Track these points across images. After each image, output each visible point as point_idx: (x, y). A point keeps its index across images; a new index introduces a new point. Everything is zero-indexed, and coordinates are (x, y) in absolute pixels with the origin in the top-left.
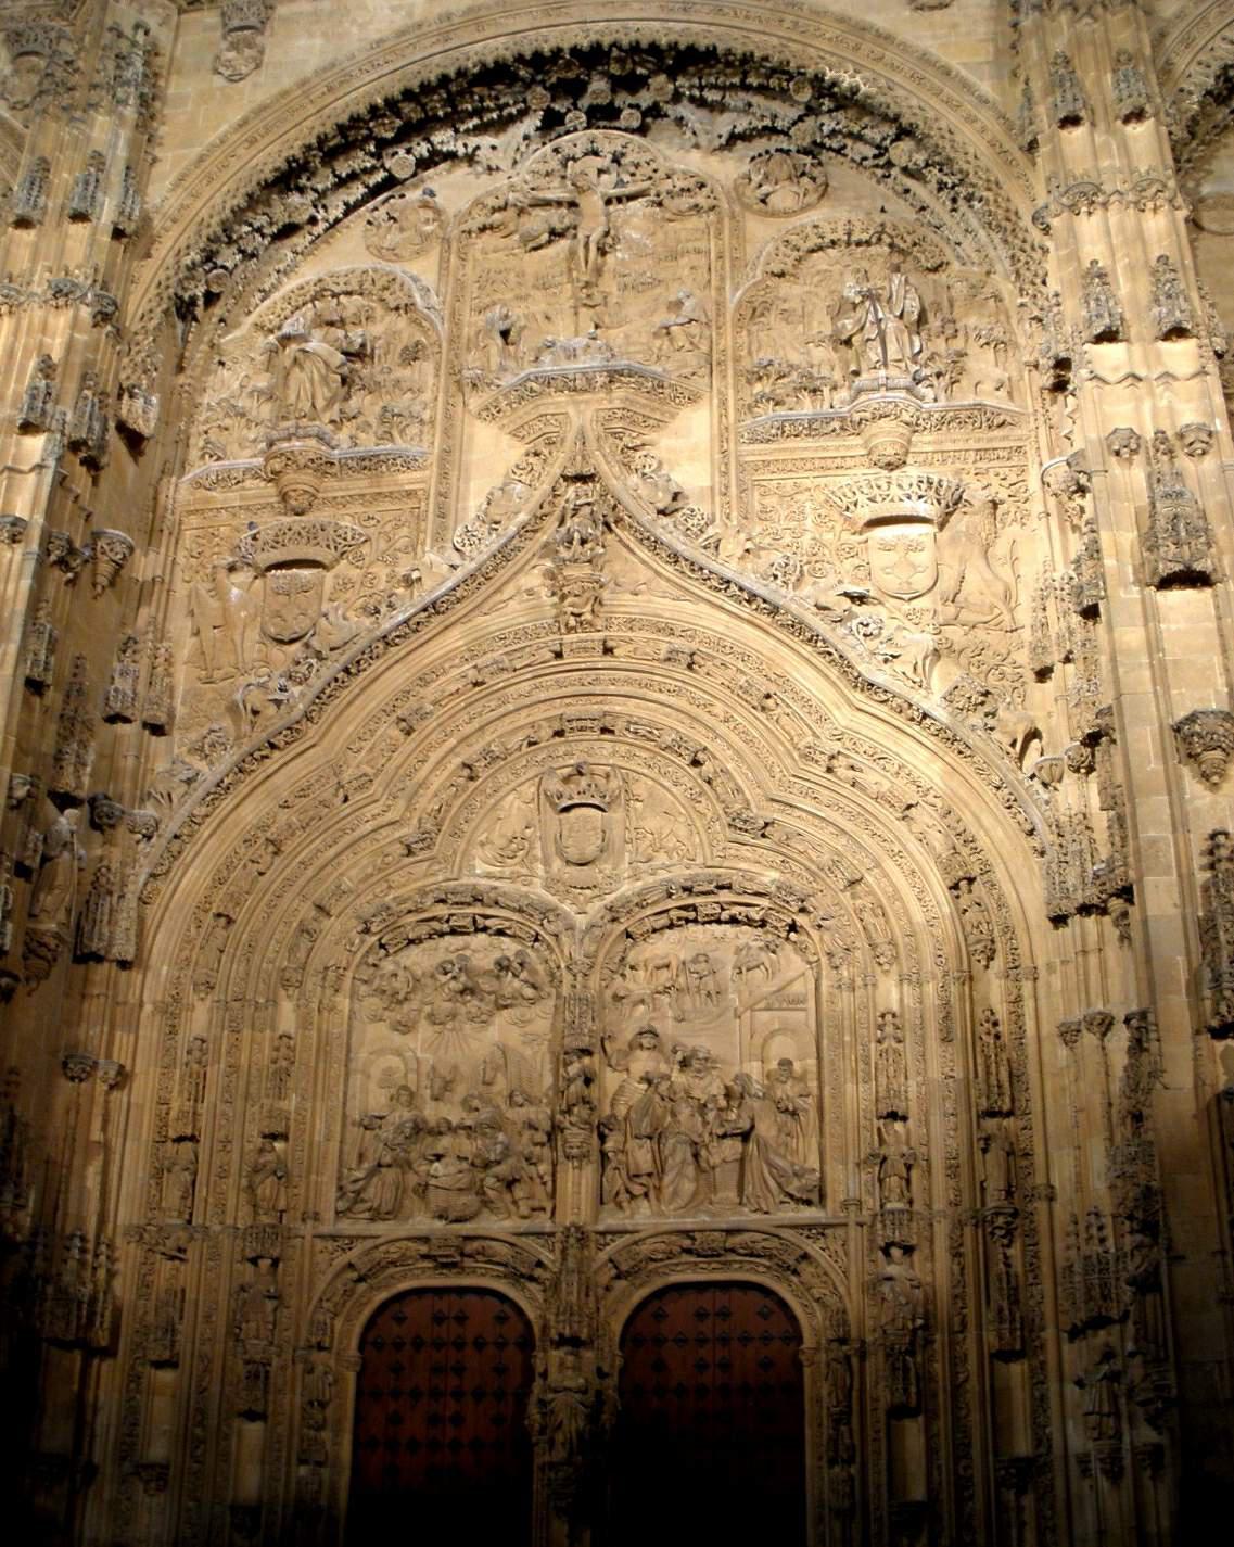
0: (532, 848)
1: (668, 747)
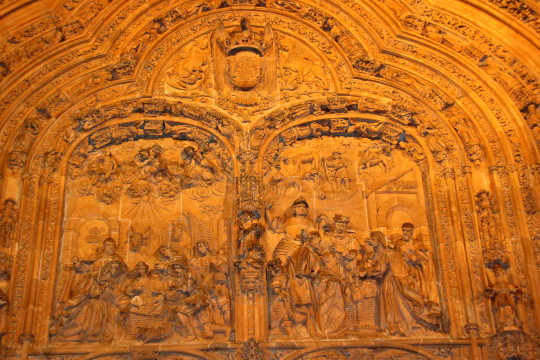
0: (207, 78)
1: (307, 15)
